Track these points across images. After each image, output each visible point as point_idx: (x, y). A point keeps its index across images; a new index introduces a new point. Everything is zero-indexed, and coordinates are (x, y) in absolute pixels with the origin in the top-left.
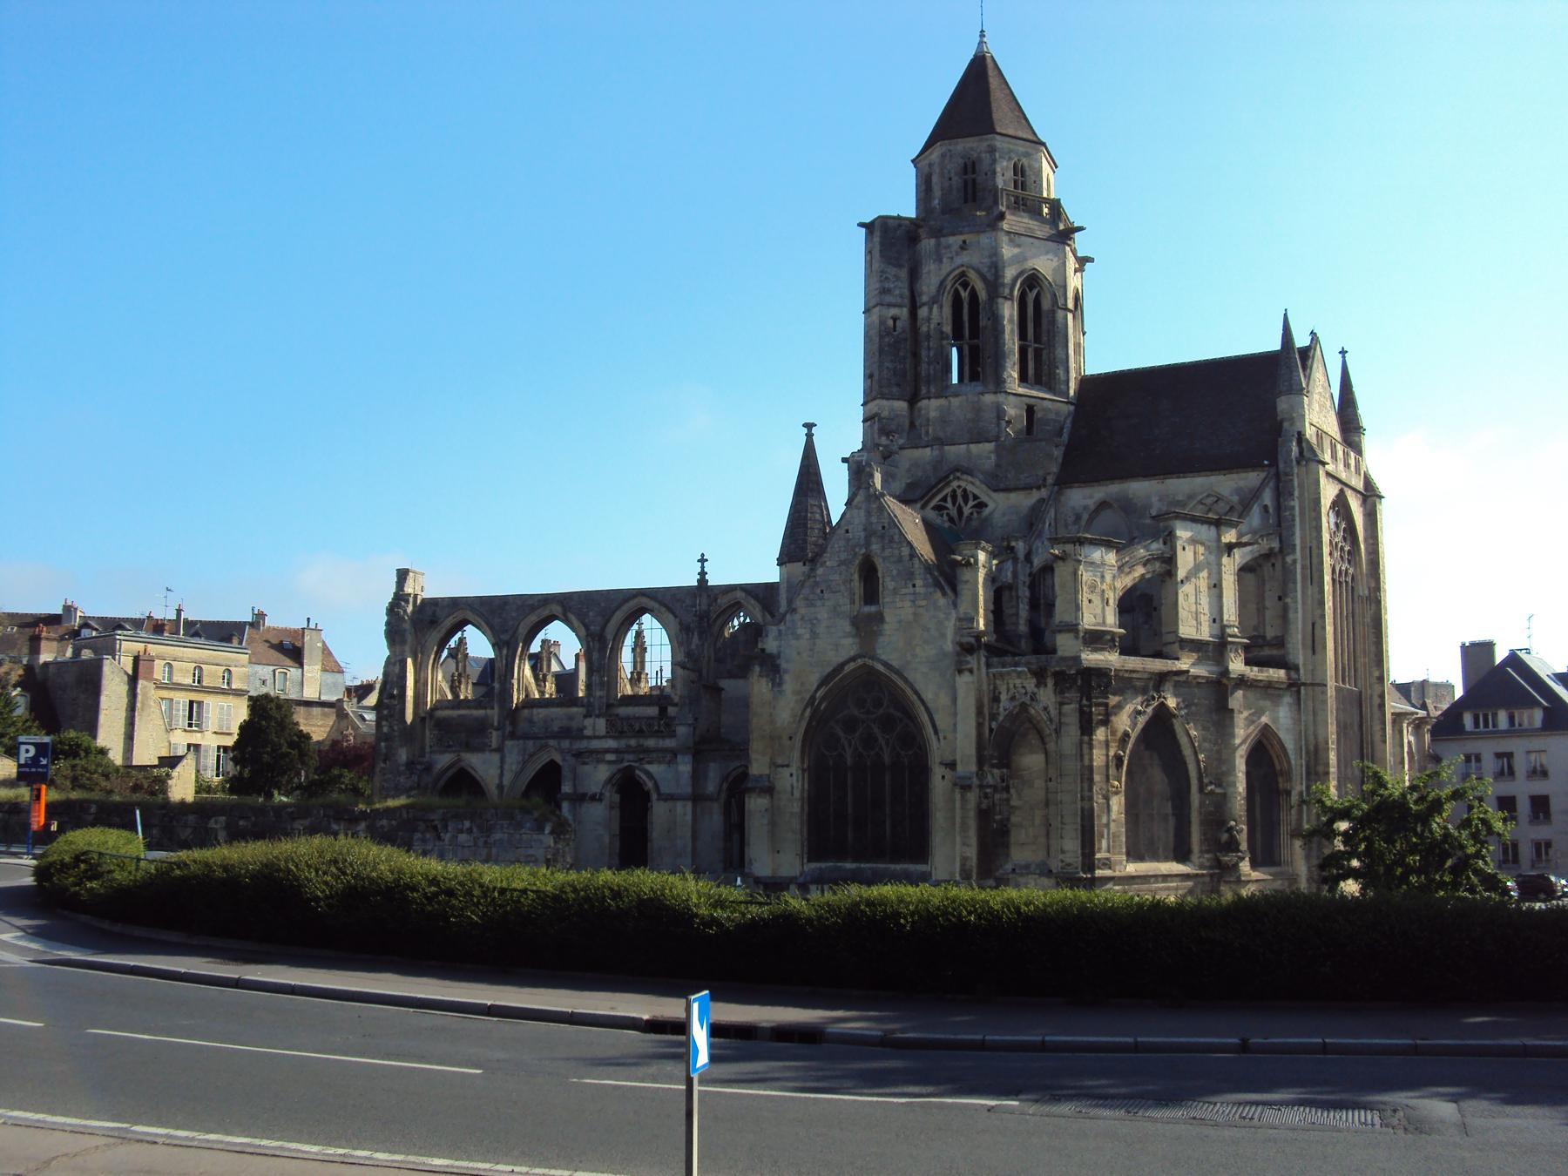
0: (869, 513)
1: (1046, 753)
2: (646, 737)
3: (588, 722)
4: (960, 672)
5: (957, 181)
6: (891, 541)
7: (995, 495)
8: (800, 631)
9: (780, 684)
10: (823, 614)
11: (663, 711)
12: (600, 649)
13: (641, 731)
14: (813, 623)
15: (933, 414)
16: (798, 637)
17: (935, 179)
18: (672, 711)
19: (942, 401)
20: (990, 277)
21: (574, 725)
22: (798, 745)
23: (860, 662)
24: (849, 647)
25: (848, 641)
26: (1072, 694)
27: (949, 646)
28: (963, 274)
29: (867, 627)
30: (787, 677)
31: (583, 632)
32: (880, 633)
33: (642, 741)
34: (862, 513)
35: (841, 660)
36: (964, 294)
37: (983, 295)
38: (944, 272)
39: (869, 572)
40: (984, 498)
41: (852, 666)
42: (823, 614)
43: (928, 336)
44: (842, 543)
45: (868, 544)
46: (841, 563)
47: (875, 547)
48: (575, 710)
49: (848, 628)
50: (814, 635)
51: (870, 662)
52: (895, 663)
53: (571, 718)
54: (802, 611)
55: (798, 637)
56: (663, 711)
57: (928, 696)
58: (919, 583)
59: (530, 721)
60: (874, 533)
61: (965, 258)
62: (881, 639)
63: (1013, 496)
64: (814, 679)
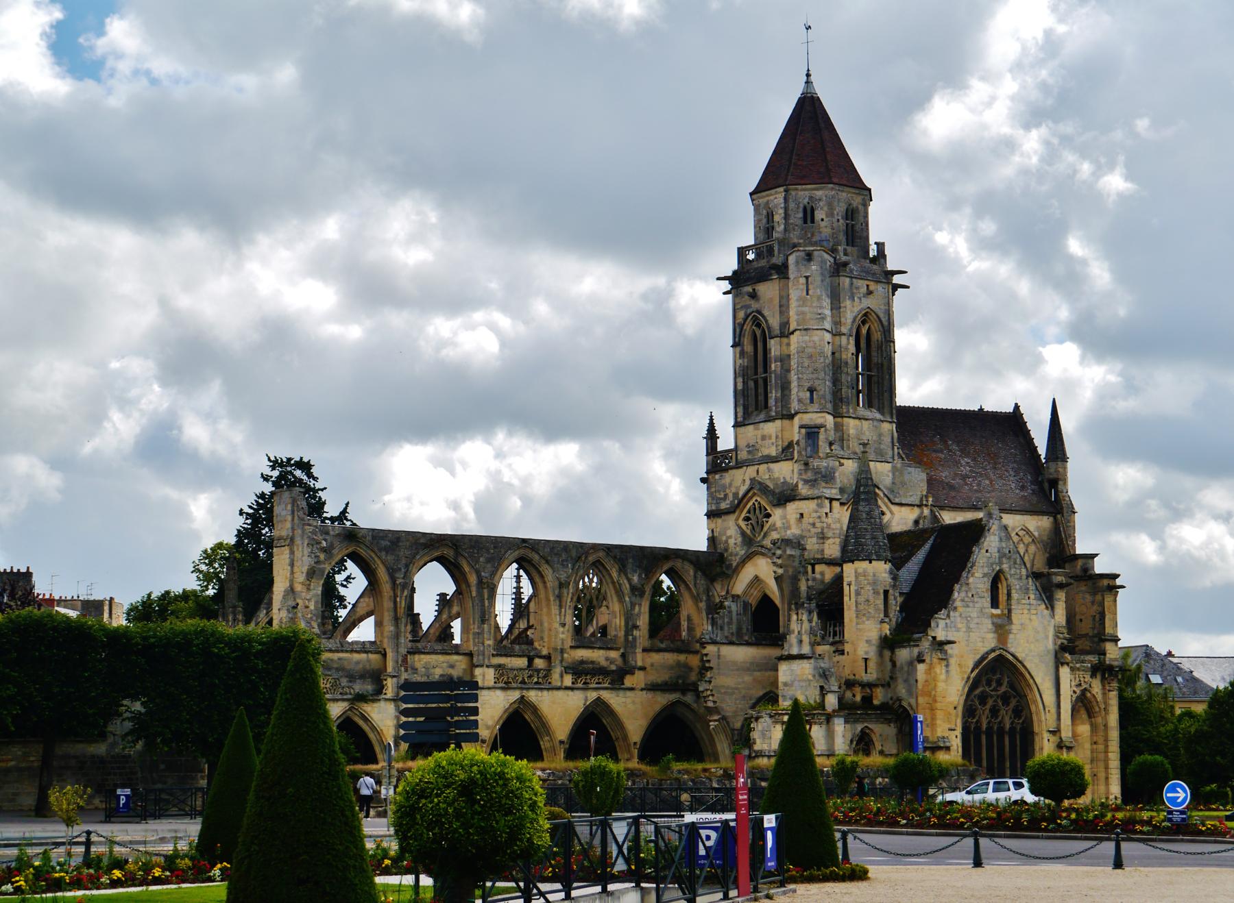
1: (1092, 725)
2: (528, 689)
3: (478, 671)
4: (1062, 664)
6: (1015, 563)
7: (895, 508)
8: (960, 626)
9: (947, 666)
10: (974, 615)
11: (531, 661)
12: (471, 595)
13: (523, 682)
14: (968, 619)
15: (852, 431)
17: (819, 214)
18: (539, 663)
19: (857, 422)
20: (886, 323)
21: (456, 673)
22: (960, 714)
23: (998, 653)
25: (991, 635)
26: (1115, 684)
27: (1050, 644)
28: (866, 315)
29: (1002, 628)
30: (952, 661)
31: (473, 579)
32: (1009, 632)
33: (525, 693)
34: (997, 538)
35: (986, 650)
36: (864, 331)
37: (877, 336)
38: (856, 310)
40: (884, 509)
41: (993, 655)
43: (846, 363)
44: (985, 560)
45: (1001, 563)
46: (985, 575)
47: (1005, 566)
48: (455, 657)
49: (990, 626)
50: (969, 629)
51: (1004, 653)
52: (1018, 655)
53: (452, 666)
54: (960, 609)
55: (958, 630)
56: (531, 661)
57: (1038, 680)
58: (1032, 596)
59: (415, 670)
60: (1005, 555)
61: (868, 302)
62: (1011, 636)
63: (903, 509)
64: (971, 666)
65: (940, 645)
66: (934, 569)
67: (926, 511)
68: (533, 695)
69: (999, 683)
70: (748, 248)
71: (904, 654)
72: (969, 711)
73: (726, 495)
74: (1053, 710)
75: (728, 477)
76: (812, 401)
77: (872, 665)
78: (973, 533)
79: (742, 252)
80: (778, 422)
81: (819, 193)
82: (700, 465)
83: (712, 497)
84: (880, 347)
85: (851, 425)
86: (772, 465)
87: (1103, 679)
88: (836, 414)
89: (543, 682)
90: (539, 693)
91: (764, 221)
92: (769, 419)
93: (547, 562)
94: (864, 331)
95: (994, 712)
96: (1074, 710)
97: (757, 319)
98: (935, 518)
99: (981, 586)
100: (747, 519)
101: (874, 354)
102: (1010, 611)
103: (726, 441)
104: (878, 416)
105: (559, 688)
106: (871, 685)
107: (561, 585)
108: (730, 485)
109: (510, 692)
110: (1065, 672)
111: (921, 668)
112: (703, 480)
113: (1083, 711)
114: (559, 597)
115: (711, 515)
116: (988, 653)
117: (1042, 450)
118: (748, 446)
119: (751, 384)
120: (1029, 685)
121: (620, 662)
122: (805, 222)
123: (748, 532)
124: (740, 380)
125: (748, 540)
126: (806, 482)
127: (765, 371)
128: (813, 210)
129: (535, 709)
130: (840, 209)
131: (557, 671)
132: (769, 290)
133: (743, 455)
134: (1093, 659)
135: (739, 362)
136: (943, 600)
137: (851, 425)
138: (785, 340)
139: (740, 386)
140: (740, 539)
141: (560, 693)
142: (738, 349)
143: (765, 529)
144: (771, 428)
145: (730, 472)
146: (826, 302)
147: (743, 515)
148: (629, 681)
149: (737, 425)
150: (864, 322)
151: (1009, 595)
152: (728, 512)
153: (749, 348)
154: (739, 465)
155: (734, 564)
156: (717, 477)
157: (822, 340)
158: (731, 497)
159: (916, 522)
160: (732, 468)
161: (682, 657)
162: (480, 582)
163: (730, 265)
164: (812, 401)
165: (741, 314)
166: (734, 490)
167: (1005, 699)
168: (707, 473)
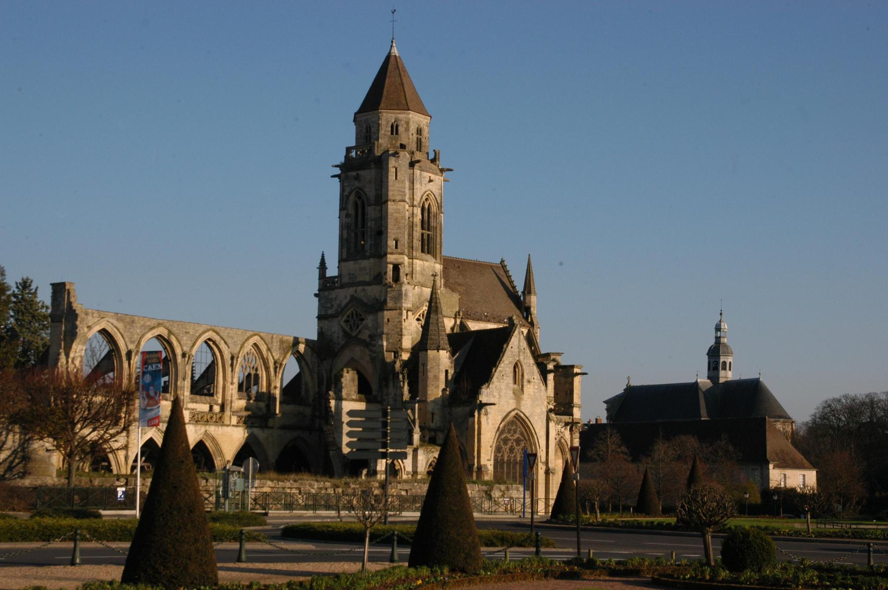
0: (519, 341)
5: (415, 136)
10: (503, 387)
14: (500, 390)
15: (418, 268)
16: (494, 397)
17: (401, 129)
19: (421, 262)
24: (512, 404)
30: (489, 416)
33: (207, 427)
35: (509, 410)
36: (426, 206)
37: (434, 209)
39: (515, 368)
41: (513, 413)
42: (503, 387)
47: (522, 358)
49: (512, 395)
50: (500, 396)
52: (527, 414)
54: (496, 384)
55: (494, 397)
64: (500, 418)
65: (482, 405)
66: (478, 356)
67: (458, 322)
68: (212, 429)
69: (515, 432)
70: (352, 148)
71: (459, 411)
72: (498, 449)
73: (332, 306)
74: (544, 450)
75: (333, 294)
76: (396, 247)
77: (437, 418)
78: (501, 337)
79: (349, 150)
80: (372, 260)
81: (402, 116)
82: (314, 286)
83: (321, 306)
84: (436, 216)
85: (418, 263)
86: (366, 287)
87: (571, 430)
88: (411, 258)
89: (220, 421)
90: (216, 428)
91: (364, 131)
92: (365, 258)
93: (226, 343)
94: (426, 206)
95: (511, 450)
96: (556, 451)
97: (360, 194)
98: (463, 326)
99: (508, 369)
100: (347, 321)
101: (432, 220)
102: (523, 386)
103: (332, 271)
104: (434, 260)
105: (228, 426)
106: (435, 430)
107: (232, 358)
108: (336, 298)
109: (199, 427)
110: (552, 424)
111: (471, 420)
112: (316, 295)
113: (560, 454)
114: (232, 365)
115: (320, 318)
116: (510, 412)
117: (520, 288)
118: (349, 274)
119: (353, 235)
120: (532, 434)
121: (264, 410)
122: (392, 133)
123: (347, 329)
124: (345, 232)
125: (346, 334)
126: (391, 298)
127: (363, 226)
128: (397, 126)
129: (213, 439)
130: (413, 128)
131: (228, 412)
132: (368, 174)
133: (346, 280)
134: (567, 418)
135: (345, 220)
136: (486, 377)
137: (418, 263)
138: (378, 208)
139: (345, 236)
140: (341, 334)
141: (230, 428)
142: (345, 212)
143: (360, 327)
144: (365, 263)
145: (336, 291)
146: (407, 184)
147: (345, 318)
148: (271, 422)
149: (341, 260)
150: (427, 199)
151: (523, 376)
152: (333, 316)
153: (351, 211)
154: (342, 286)
155: (337, 350)
156: (326, 293)
157: (404, 207)
158: (335, 306)
159: (452, 329)
160: (338, 288)
161: (301, 408)
162: (184, 355)
163: (341, 159)
164: (396, 247)
165: (348, 190)
166: (338, 302)
167: (518, 441)
168: (319, 290)
